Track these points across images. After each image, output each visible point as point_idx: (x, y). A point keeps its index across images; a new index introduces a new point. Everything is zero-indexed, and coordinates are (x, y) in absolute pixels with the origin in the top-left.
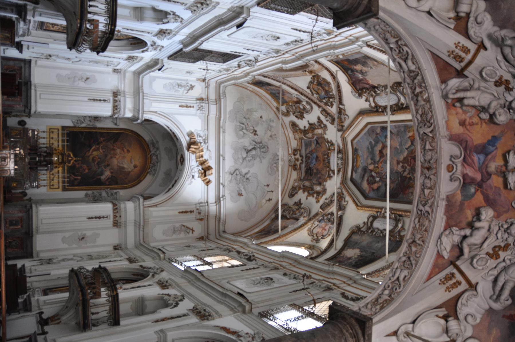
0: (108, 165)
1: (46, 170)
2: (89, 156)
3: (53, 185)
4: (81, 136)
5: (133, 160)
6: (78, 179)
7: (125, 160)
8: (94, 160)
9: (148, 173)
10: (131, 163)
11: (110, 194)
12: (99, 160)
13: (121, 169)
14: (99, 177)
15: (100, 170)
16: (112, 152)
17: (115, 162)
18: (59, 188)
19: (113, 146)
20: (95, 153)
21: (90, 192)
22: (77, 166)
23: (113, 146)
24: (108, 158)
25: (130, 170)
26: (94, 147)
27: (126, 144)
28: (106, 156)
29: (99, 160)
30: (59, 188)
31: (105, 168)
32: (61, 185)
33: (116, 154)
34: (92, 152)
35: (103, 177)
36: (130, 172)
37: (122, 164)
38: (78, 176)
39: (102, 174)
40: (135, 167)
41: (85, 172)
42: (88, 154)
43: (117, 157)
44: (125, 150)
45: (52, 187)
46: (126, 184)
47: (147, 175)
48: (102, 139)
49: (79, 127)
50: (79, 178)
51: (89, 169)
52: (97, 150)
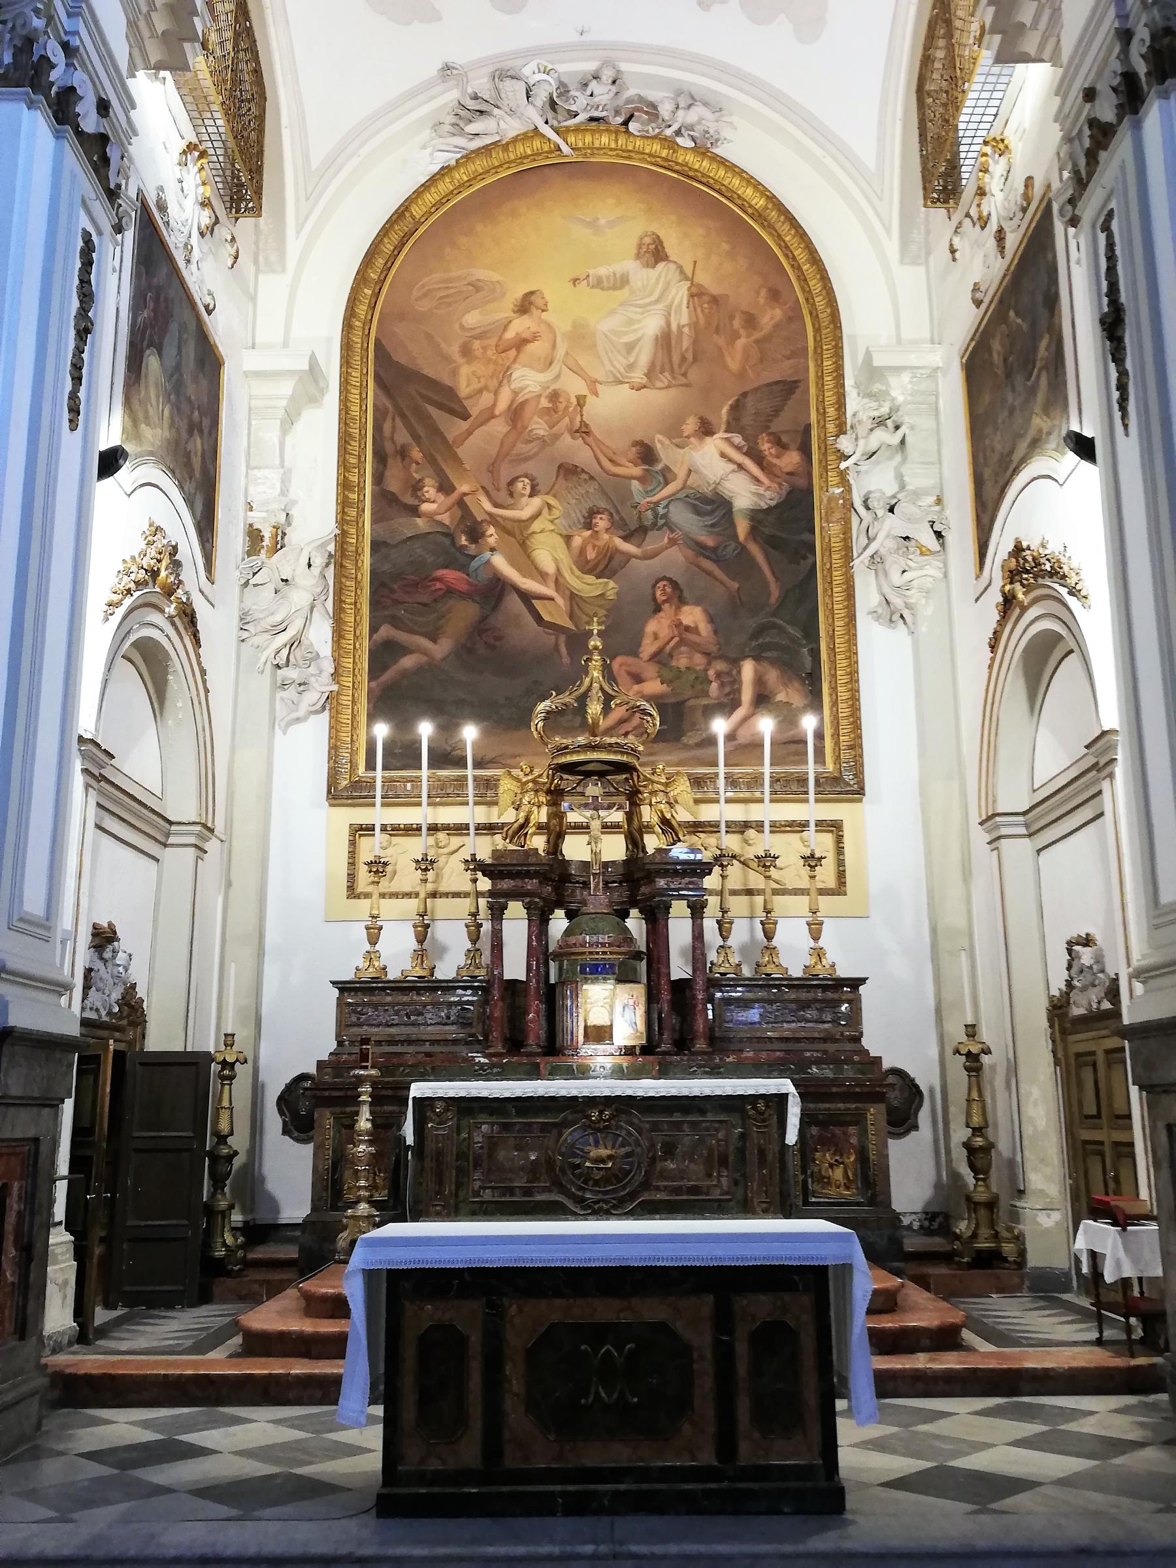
0: (647, 455)
1: (697, 910)
2: (573, 597)
3: (812, 861)
4: (408, 662)
5: (603, 271)
6: (759, 681)
7: (605, 326)
8: (606, 565)
9: (701, 150)
10: (622, 282)
11: (882, 436)
12: (601, 522)
13: (671, 358)
14: (742, 528)
15: (681, 516)
16: (539, 427)
17: (619, 405)
18: (834, 827)
19: (489, 415)
20: (546, 555)
21: (867, 595)
22: (654, 686)
23: (489, 415)
24: (582, 455)
25: (680, 293)
26: (500, 562)
27: (472, 319)
28: (569, 471)
29: (601, 522)
30: (834, 827)
31: (667, 476)
32: (810, 810)
33: (554, 396)
34: (542, 576)
35: (745, 493)
36: (697, 293)
37: (630, 347)
38: (732, 683)
39: (714, 505)
40: (655, 253)
41: (705, 628)
42: (556, 612)
43: (574, 386)
44: (520, 326)
45: (826, 875)
46: (794, 316)
47: (723, 162)
48: (434, 504)
49: (336, 675)
50: (748, 670)
51: (680, 598)
52: (518, 537)
